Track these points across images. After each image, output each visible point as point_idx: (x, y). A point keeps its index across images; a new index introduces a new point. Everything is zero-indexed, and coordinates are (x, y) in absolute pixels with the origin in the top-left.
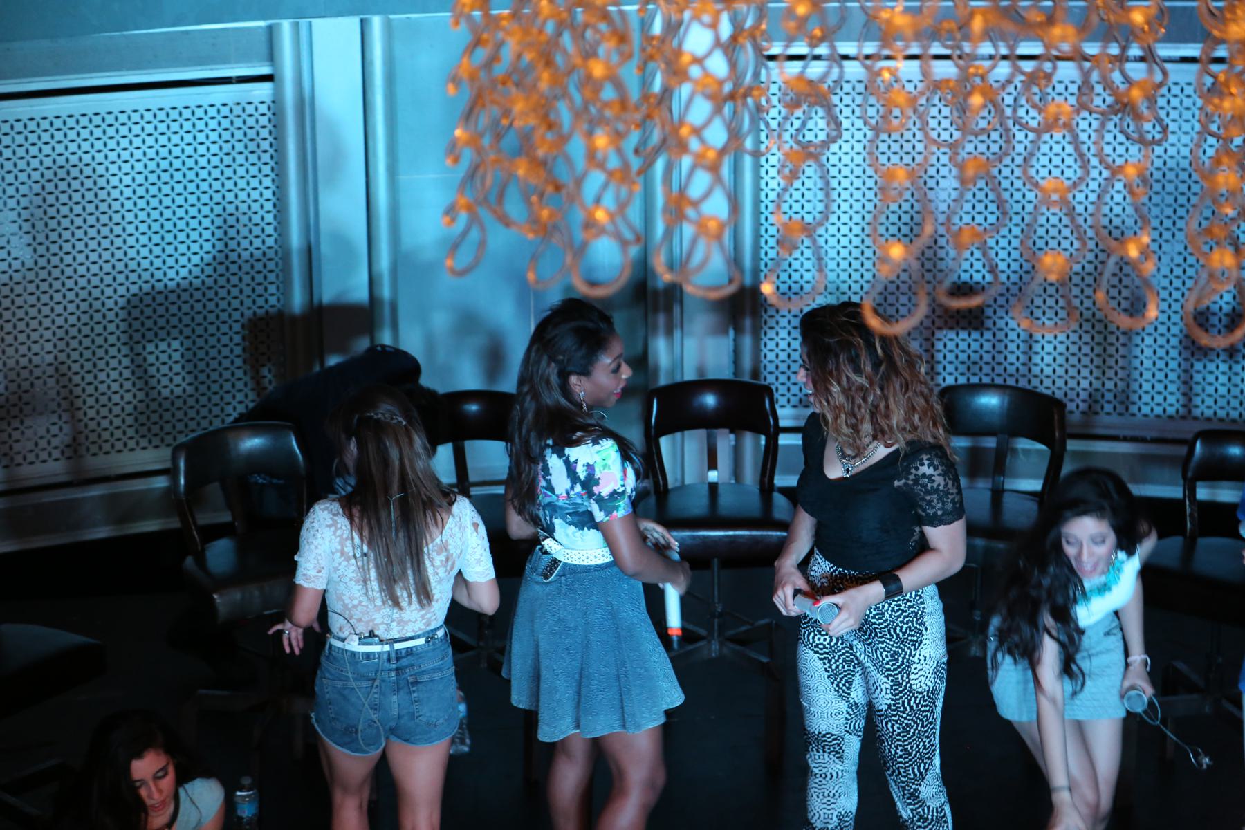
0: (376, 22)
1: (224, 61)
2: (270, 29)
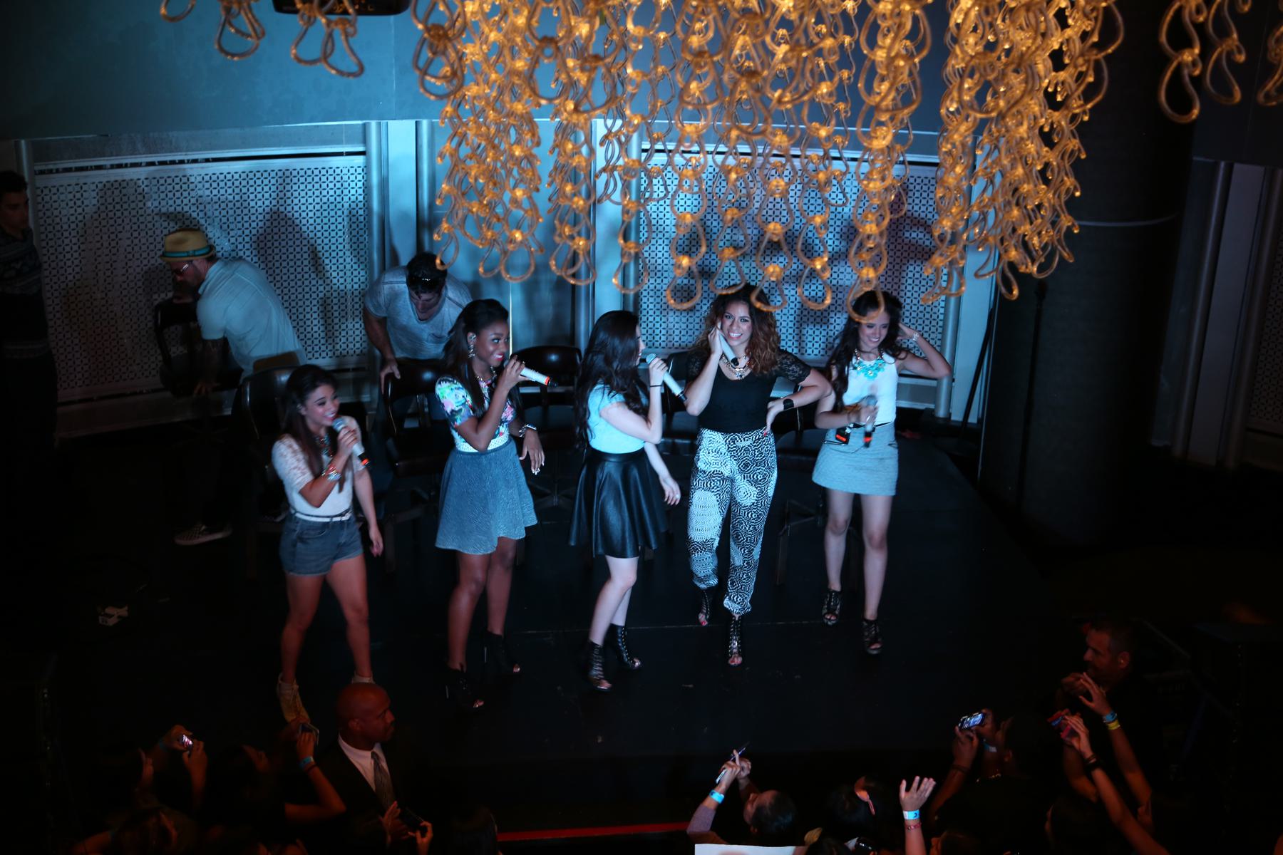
0: (425, 124)
1: (339, 142)
2: (364, 125)
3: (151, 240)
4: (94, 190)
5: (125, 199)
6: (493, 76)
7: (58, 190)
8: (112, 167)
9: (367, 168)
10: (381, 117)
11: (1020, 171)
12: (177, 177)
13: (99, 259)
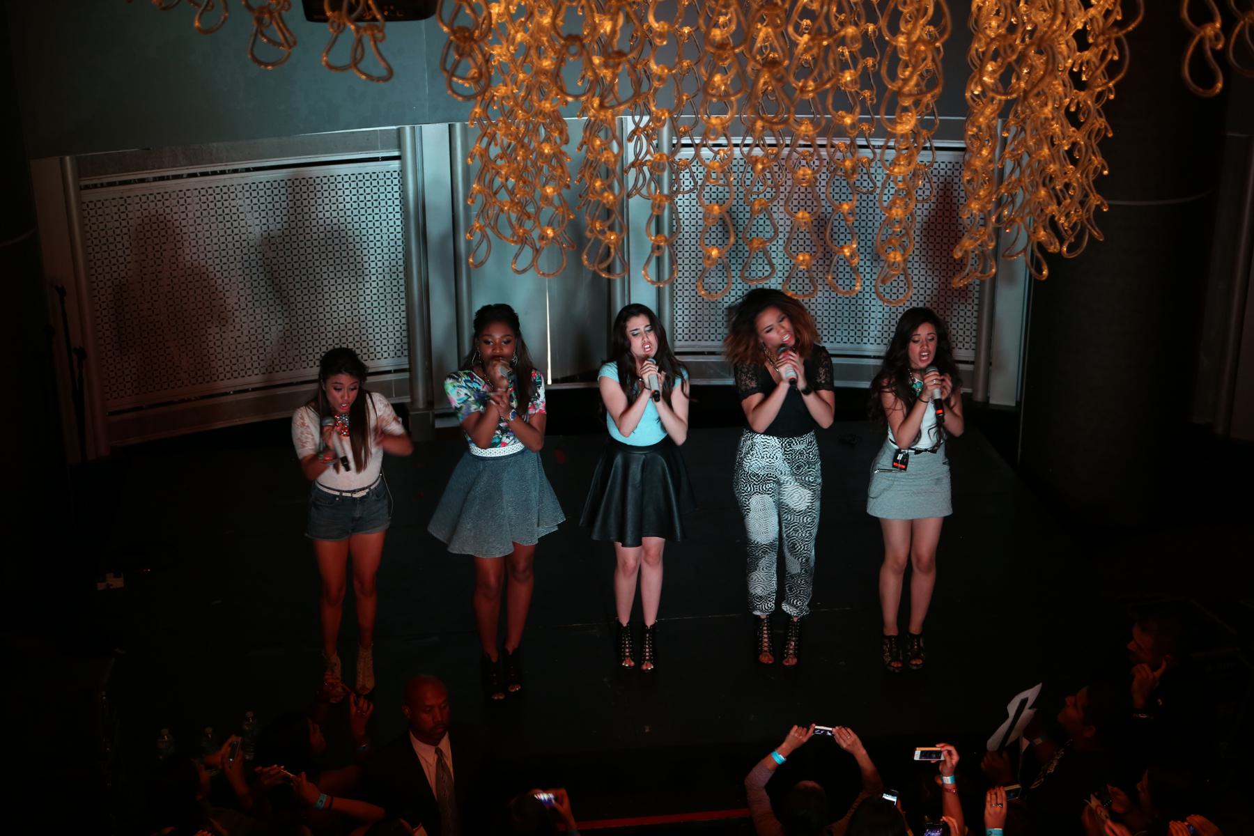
0: (458, 126)
1: (375, 148)
2: (399, 130)
3: (194, 250)
4: (138, 203)
5: (168, 210)
6: (521, 76)
7: (103, 204)
8: (155, 179)
9: (402, 173)
10: (415, 121)
11: (1046, 151)
12: (217, 187)
13: (145, 271)
